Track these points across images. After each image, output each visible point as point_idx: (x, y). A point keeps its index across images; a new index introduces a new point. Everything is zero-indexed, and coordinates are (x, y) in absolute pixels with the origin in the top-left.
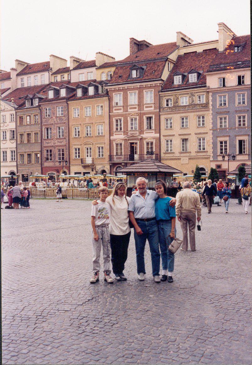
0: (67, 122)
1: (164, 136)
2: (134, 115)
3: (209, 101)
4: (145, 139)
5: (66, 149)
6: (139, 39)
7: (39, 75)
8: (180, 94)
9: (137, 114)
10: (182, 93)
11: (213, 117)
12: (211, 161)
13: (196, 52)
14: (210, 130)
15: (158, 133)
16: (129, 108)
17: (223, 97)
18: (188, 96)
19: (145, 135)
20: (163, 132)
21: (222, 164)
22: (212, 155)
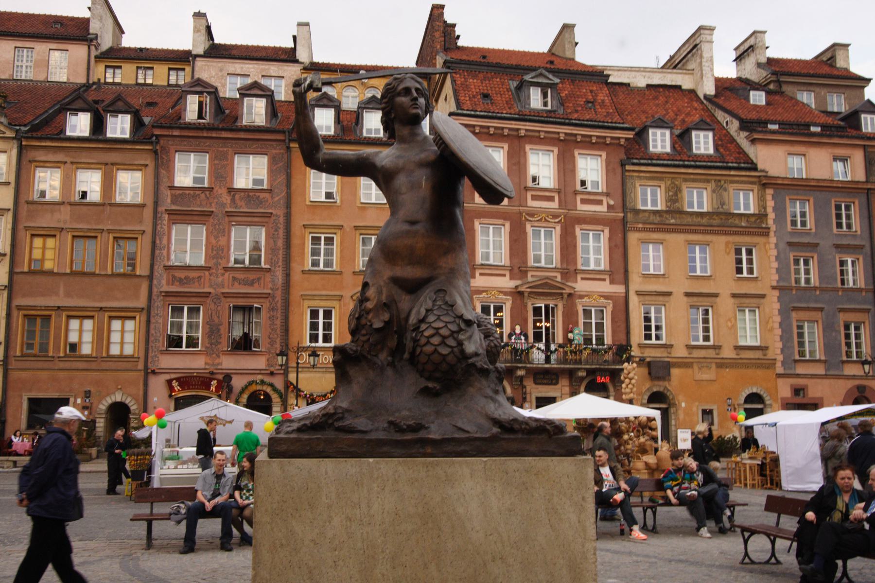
0: (280, 212)
1: (639, 293)
2: (546, 221)
3: (765, 208)
4: (581, 297)
5: (272, 309)
6: (449, 17)
7: (41, 47)
8: (686, 180)
9: (555, 216)
10: (692, 176)
11: (778, 253)
12: (779, 376)
13: (629, 84)
14: (774, 288)
15: (620, 283)
16: (529, 197)
17: (798, 203)
18: (709, 189)
19: (581, 286)
20: (636, 283)
21: (807, 386)
22: (780, 358)
